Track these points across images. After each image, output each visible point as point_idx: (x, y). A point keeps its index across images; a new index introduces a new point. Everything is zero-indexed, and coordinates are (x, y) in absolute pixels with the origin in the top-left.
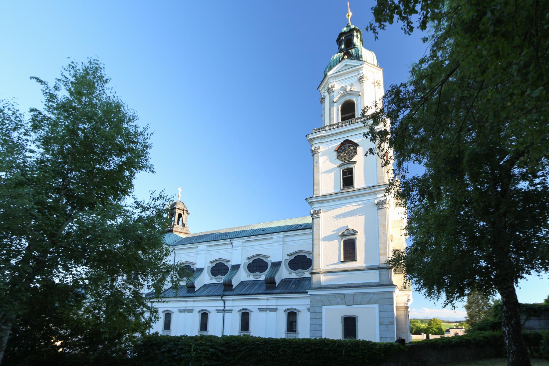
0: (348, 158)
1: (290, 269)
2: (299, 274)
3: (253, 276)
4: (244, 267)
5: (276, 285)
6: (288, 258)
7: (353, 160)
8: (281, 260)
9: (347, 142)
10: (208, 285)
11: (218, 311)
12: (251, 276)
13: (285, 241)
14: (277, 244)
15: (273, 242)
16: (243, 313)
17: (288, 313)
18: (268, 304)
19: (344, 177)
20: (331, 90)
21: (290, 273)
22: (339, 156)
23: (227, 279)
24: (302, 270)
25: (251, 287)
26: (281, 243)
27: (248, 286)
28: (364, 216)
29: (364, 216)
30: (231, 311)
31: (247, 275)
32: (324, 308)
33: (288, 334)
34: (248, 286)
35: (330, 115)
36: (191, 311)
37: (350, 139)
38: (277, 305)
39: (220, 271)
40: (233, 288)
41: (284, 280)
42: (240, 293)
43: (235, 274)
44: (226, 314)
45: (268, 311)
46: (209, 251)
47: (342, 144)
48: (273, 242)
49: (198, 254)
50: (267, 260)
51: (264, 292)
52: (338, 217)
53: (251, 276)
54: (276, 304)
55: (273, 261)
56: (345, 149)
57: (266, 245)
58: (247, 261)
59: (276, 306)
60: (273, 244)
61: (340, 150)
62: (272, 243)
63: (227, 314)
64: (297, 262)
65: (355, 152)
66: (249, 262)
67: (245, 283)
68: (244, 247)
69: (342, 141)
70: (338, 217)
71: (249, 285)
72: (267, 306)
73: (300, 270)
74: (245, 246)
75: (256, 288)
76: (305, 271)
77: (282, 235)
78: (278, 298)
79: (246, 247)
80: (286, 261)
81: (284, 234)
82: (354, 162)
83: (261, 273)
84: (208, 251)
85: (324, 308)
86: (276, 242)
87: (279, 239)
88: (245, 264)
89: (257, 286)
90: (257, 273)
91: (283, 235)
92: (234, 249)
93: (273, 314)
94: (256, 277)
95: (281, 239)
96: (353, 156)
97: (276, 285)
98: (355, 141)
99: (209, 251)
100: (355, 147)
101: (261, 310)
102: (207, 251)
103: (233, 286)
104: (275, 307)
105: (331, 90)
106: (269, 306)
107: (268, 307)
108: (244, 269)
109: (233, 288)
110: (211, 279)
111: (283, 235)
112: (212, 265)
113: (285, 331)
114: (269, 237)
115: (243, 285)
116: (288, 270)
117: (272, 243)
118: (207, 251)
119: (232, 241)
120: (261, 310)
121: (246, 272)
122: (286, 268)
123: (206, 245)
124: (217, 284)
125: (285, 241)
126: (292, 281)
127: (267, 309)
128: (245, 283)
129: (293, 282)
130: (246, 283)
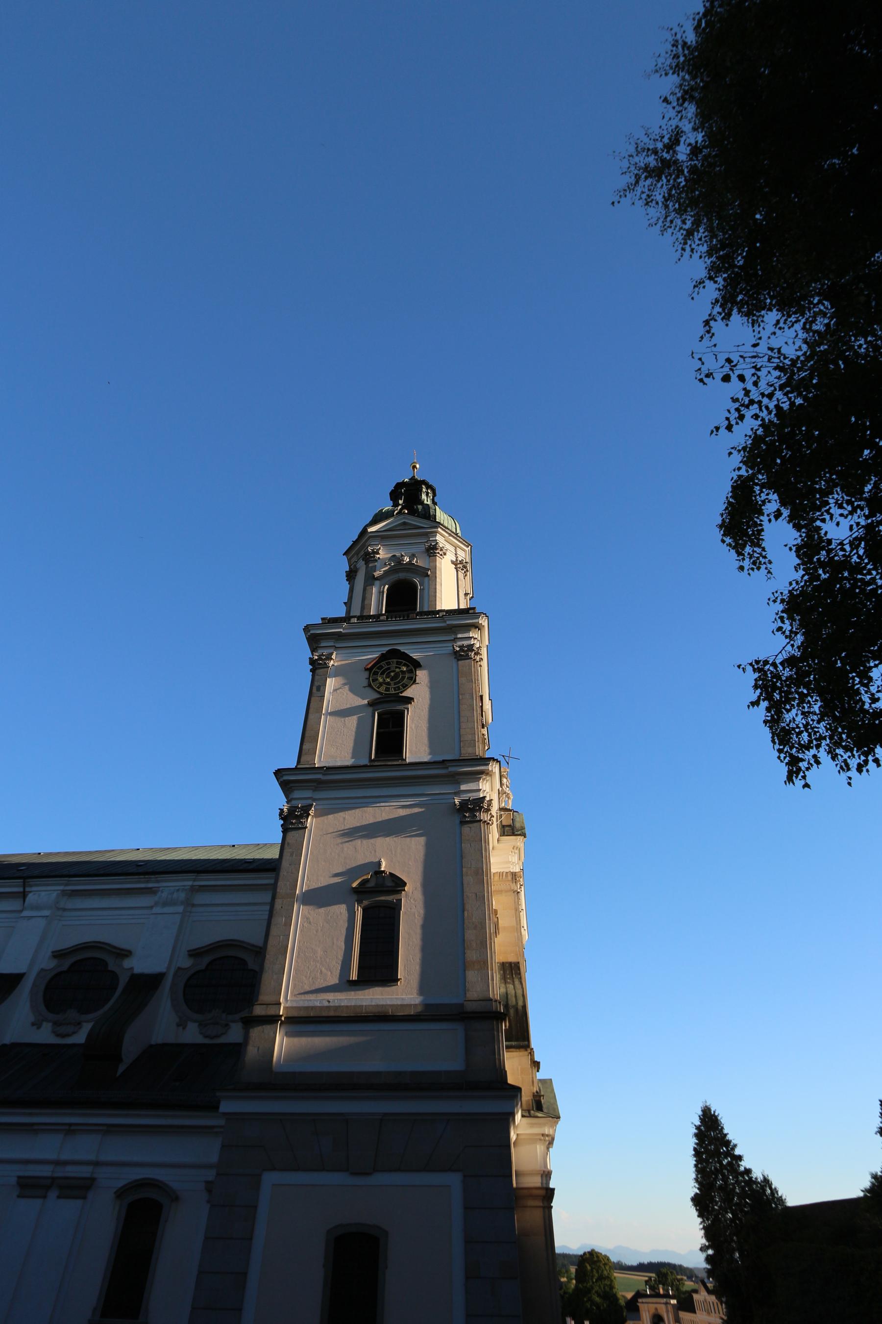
0: (394, 688)
5: (121, 1068)
7: (405, 694)
9: (394, 654)
13: (193, 905)
14: (167, 910)
15: (156, 904)
18: (64, 1157)
19: (382, 730)
20: (372, 557)
22: (373, 681)
26: (180, 909)
28: (422, 840)
29: (422, 840)
32: (270, 1179)
35: (364, 599)
37: (402, 649)
45: (53, 1194)
47: (383, 657)
48: (156, 904)
52: (352, 834)
54: (92, 1157)
55: (138, 970)
56: (389, 668)
57: (131, 912)
59: (89, 1169)
60: (155, 910)
61: (378, 668)
62: (152, 907)
65: (410, 678)
69: (385, 649)
70: (352, 834)
72: (58, 1163)
77: (186, 882)
78: (109, 1130)
81: (194, 880)
82: (409, 700)
85: (270, 1179)
86: (165, 904)
87: (175, 895)
91: (190, 883)
95: (182, 896)
96: (406, 687)
97: (121, 1068)
98: (415, 655)
100: (411, 667)
104: (84, 1171)
105: (372, 557)
106: (66, 1163)
107: (60, 1172)
111: (190, 883)
114: (150, 885)
117: (152, 907)
125: (193, 905)
127: (53, 1179)
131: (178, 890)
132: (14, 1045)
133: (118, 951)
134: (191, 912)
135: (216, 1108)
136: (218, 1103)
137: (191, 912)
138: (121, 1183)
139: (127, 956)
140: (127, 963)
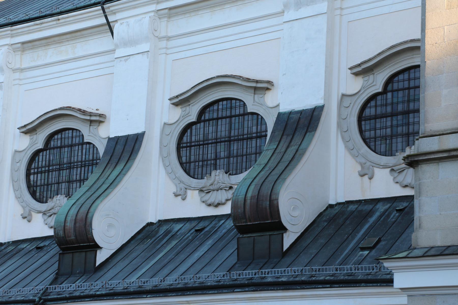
3: (201, 191)
4: (162, 146)
8: (320, 102)
10: (11, 248)
12: (189, 192)
25: (187, 245)
27: (168, 248)
31: (174, 189)
34: (168, 248)
39: (65, 173)
40: (101, 257)
41: (337, 209)
42: (120, 288)
43: (113, 184)
46: (22, 70)
50: (262, 105)
51: (226, 280)
53: (189, 192)
55: (285, 108)
58: (177, 113)
64: (400, 108)
66: (183, 117)
67: (162, 230)
68: (163, 44)
71: (174, 243)
74: (168, 38)
75: (204, 248)
79: (172, 43)
84: (17, 75)
88: (168, 130)
89: (210, 242)
92: (120, 52)
99: (22, 70)
102: (15, 70)
103: (96, 247)
109: (101, 257)
115: (150, 241)
116: (355, 157)
118: (15, 70)
121: (170, 173)
122: (346, 142)
123: (8, 41)
124: (47, 243)
126: (370, 213)
128: (162, 230)
129: (372, 220)
130: (167, 232)
132: (162, 223)
133: (254, 85)
134: (341, 9)
135: (389, 282)
136: (391, 274)
137: (341, 9)
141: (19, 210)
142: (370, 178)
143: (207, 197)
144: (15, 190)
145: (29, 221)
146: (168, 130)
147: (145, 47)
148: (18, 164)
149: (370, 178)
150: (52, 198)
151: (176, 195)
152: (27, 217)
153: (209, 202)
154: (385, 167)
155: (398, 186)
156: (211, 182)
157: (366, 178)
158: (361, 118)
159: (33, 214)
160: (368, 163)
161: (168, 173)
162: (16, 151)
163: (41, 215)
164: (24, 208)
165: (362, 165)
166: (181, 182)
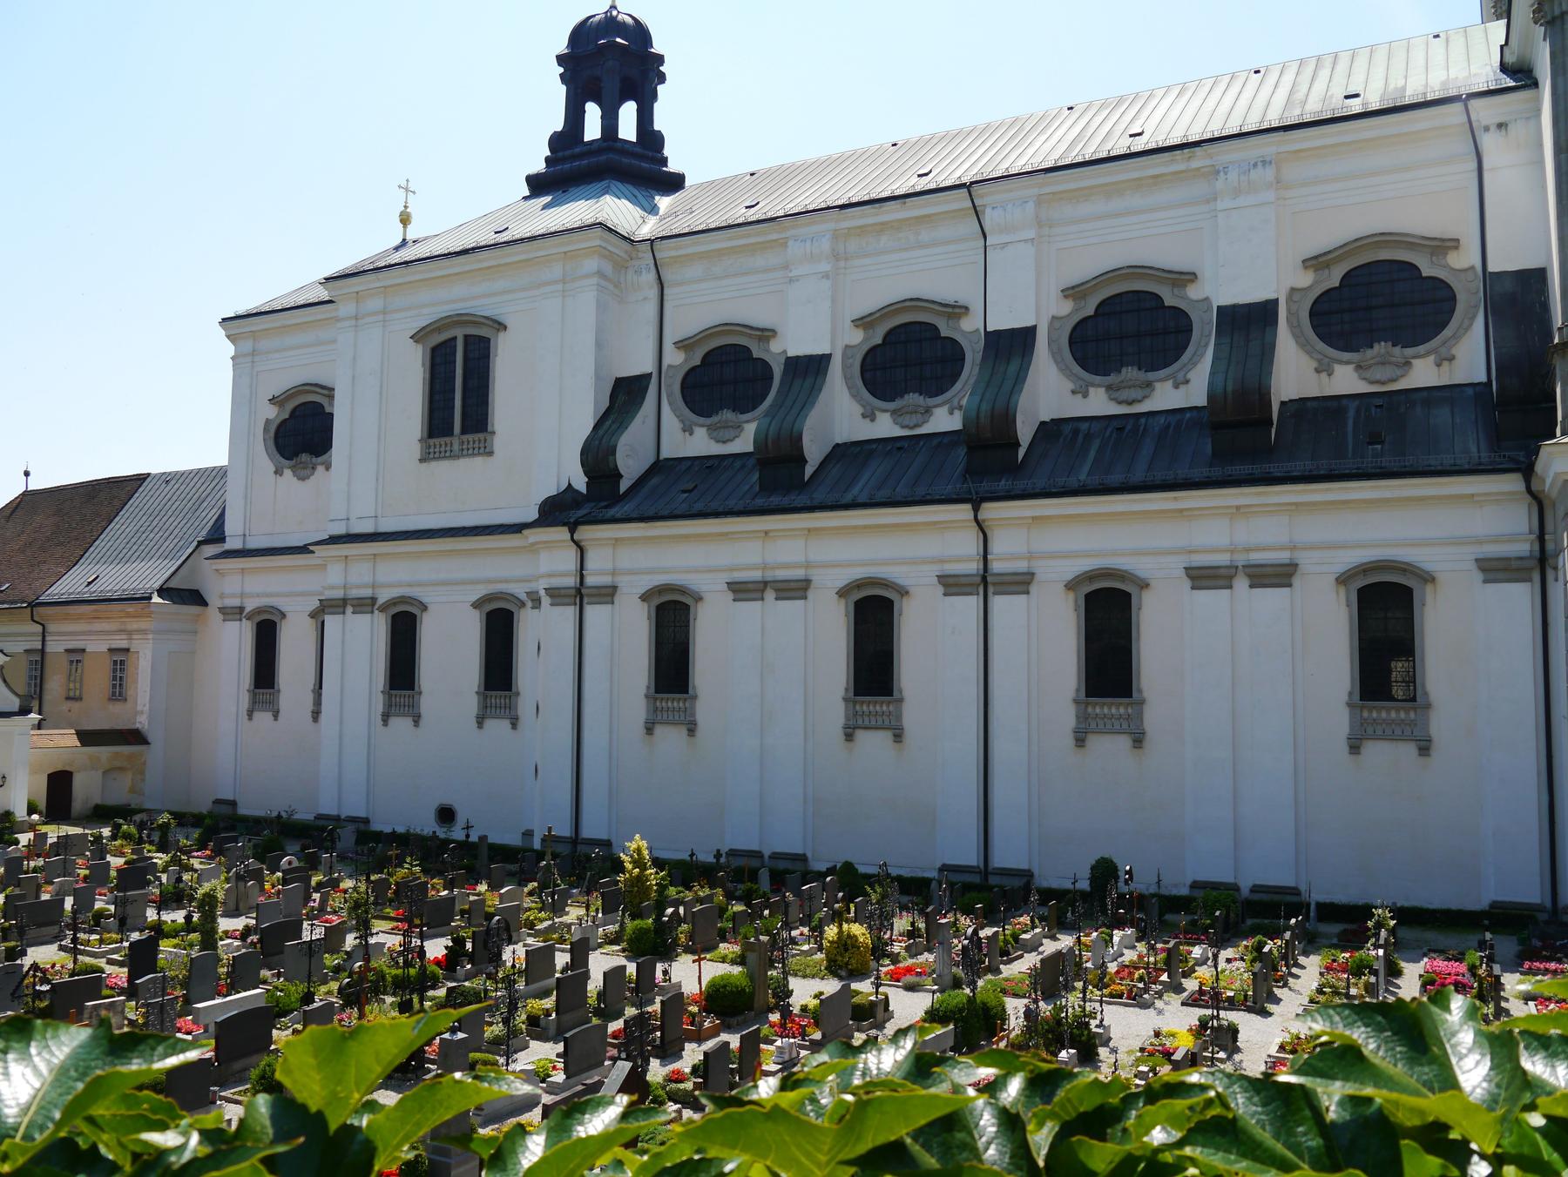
1: (1321, 345)
2: (1379, 373)
6: (1305, 279)
11: (952, 585)
12: (1091, 390)
16: (1090, 598)
17: (1361, 592)
21: (1324, 368)
23: (984, 407)
24: (1397, 350)
26: (1270, 195)
30: (1021, 583)
31: (1071, 386)
33: (1362, 708)
36: (796, 589)
38: (1293, 548)
44: (999, 603)
49: (791, 280)
50: (1185, 298)
53: (1091, 390)
63: (999, 603)
73: (1380, 348)
76: (1409, 351)
80: (1296, 297)
83: (1151, 376)
88: (1057, 325)
90: (1130, 373)
93: (1272, 599)
94: (1125, 394)
101: (1204, 577)
108: (1055, 354)
110: (870, 416)
112: (865, 340)
113: (1350, 694)
119: (982, 196)
120: (1204, 577)
131: (1255, 165)
138: (1341, 568)
139: (1192, 281)
140: (1194, 292)
141: (857, 410)
142: (1329, 375)
143: (1116, 395)
144: (849, 388)
145: (873, 420)
146: (1057, 325)
147: (1031, 234)
148: (851, 361)
149: (1329, 375)
150: (902, 396)
151: (1074, 392)
152: (870, 416)
153: (1121, 399)
154: (1348, 363)
155: (1364, 382)
156: (1120, 379)
157: (1324, 375)
158: (1313, 314)
159: (877, 413)
160: (1327, 360)
161: (1061, 370)
162: (847, 346)
163: (887, 415)
164: (863, 406)
165: (1319, 361)
166: (1082, 379)
